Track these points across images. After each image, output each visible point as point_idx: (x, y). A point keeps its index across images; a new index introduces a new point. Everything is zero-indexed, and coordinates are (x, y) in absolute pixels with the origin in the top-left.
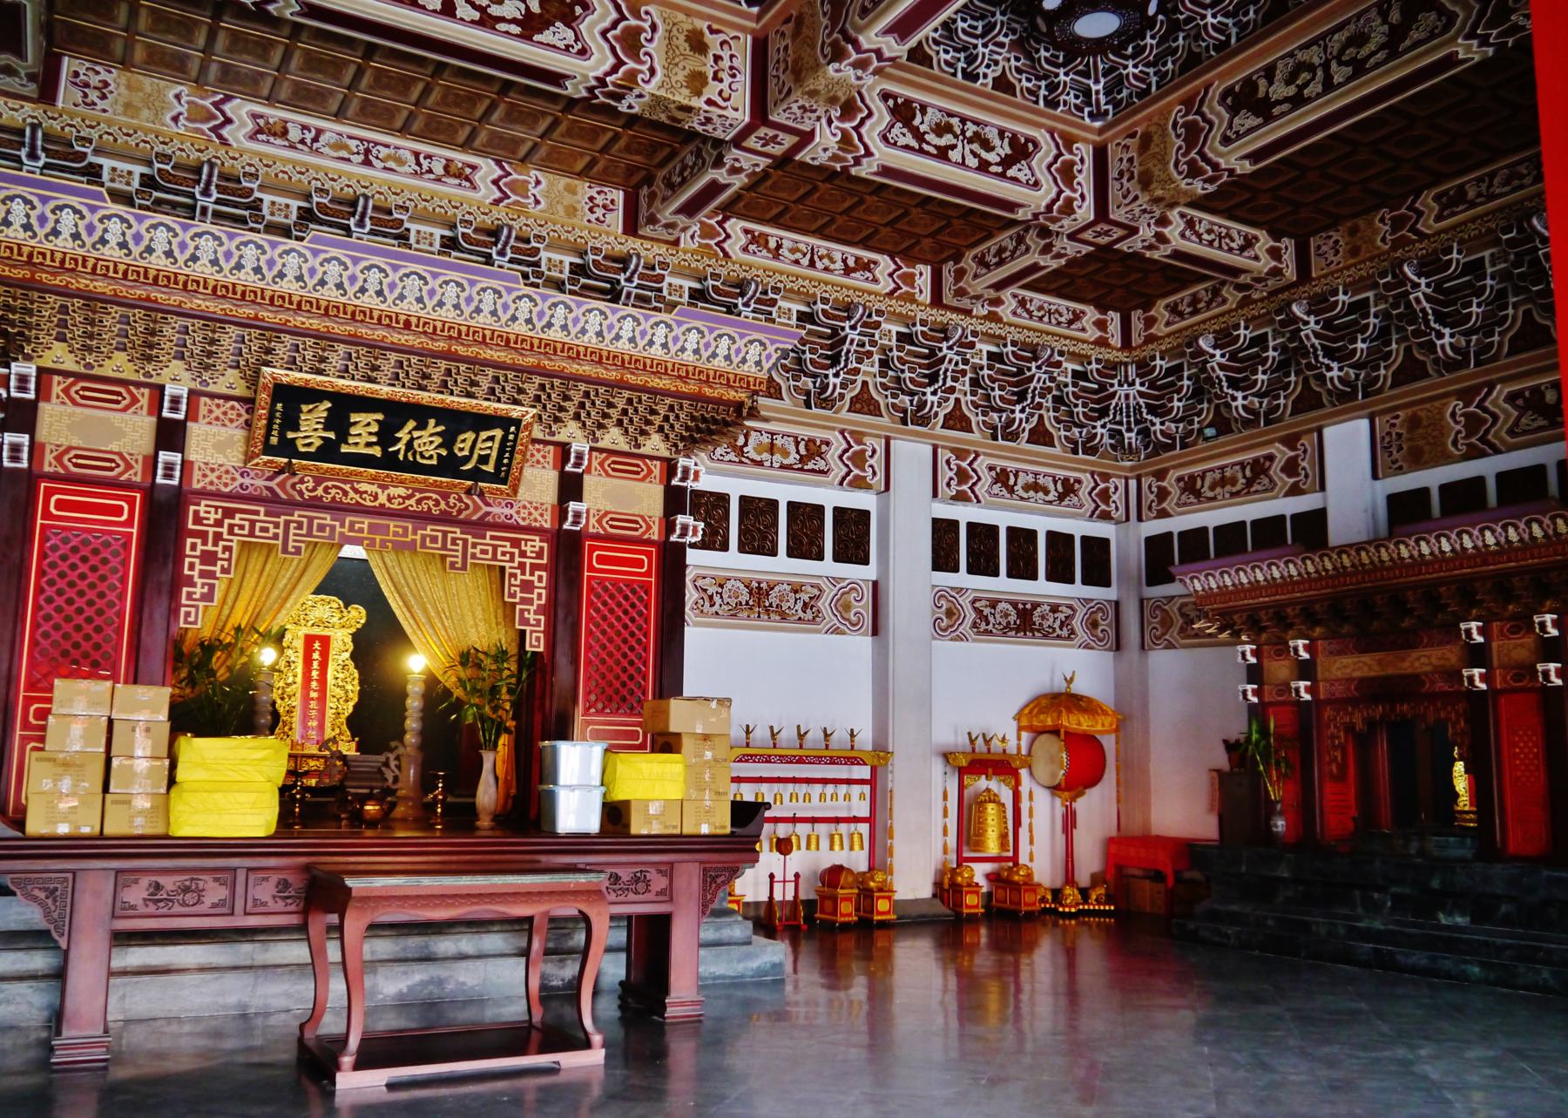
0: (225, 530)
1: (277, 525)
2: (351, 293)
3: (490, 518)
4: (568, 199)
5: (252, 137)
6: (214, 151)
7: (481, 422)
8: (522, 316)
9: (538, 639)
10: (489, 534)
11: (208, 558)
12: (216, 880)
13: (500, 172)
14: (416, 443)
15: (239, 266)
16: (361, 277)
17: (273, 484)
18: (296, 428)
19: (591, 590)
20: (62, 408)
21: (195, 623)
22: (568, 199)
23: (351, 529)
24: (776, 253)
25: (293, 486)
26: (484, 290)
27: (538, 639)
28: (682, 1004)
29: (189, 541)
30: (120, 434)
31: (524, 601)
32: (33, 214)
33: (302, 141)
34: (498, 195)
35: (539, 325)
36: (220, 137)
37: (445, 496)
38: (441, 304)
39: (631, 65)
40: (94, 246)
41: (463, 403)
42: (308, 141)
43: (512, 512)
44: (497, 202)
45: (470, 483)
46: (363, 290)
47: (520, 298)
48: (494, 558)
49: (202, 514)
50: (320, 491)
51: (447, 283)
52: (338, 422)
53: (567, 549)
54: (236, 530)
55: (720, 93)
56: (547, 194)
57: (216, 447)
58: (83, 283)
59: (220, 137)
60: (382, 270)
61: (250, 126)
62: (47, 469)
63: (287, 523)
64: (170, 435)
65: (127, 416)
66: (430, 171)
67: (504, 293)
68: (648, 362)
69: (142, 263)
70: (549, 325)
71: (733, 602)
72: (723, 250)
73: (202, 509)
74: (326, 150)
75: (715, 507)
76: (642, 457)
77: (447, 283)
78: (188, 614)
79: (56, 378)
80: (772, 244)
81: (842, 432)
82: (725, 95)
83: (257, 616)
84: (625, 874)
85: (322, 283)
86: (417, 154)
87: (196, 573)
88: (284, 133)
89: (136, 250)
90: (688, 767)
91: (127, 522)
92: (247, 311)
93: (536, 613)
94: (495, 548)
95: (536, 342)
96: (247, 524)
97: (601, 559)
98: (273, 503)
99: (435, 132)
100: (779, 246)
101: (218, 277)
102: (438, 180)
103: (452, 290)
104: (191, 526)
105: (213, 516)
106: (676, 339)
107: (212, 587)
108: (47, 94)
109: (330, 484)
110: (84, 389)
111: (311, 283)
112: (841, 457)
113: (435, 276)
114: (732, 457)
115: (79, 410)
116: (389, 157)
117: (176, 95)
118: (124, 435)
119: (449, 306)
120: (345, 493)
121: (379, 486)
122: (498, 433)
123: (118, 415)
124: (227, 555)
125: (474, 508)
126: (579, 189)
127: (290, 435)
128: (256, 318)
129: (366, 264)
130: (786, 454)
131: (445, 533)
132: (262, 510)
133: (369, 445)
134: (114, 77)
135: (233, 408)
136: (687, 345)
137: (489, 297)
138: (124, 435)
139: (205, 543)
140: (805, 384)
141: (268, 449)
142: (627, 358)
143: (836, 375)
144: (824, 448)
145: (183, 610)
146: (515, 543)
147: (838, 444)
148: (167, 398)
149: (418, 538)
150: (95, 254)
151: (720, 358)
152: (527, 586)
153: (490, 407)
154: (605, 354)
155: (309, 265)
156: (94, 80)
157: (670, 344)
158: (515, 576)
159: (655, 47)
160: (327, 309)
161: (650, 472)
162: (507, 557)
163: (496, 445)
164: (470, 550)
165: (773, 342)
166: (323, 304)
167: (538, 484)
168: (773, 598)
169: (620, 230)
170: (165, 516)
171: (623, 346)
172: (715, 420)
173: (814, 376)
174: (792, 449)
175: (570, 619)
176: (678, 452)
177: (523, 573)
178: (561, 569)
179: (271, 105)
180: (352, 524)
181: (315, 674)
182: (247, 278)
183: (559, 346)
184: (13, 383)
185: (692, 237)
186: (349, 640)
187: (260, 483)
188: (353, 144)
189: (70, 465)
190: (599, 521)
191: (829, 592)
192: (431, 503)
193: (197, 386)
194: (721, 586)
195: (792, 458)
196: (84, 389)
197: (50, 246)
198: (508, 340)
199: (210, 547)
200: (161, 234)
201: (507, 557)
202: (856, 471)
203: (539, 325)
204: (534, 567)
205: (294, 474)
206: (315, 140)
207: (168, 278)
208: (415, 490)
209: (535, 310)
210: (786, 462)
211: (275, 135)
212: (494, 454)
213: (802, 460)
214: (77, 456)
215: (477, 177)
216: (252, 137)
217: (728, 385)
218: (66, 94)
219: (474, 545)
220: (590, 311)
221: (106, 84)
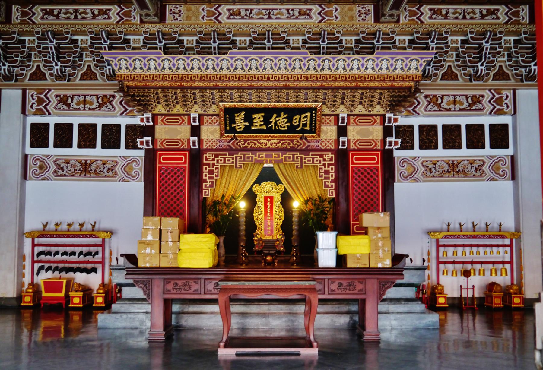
0: (215, 162)
1: (233, 158)
2: (247, 70)
3: (310, 148)
4: (350, 14)
5: (229, 18)
6: (217, 27)
7: (301, 111)
9: (332, 192)
10: (310, 153)
11: (211, 172)
12: (195, 282)
13: (320, 9)
14: (278, 123)
15: (207, 68)
16: (249, 64)
17: (230, 144)
18: (235, 123)
19: (353, 171)
20: (162, 126)
21: (208, 195)
22: (350, 14)
23: (259, 157)
24: (446, 17)
25: (237, 144)
26: (295, 60)
27: (332, 192)
28: (371, 334)
29: (204, 167)
30: (180, 133)
31: (325, 178)
32: (142, 64)
33: (246, 15)
35: (319, 70)
36: (218, 20)
37: (292, 141)
38: (280, 68)
40: (161, 70)
42: (248, 14)
43: (319, 144)
44: (320, 21)
45: (301, 135)
46: (251, 69)
47: (310, 60)
48: (313, 162)
49: (208, 157)
50: (246, 145)
51: (281, 60)
52: (249, 118)
53: (342, 157)
54: (219, 162)
56: (341, 13)
57: (211, 133)
58: (161, 84)
59: (218, 20)
60: (256, 60)
61: (228, 14)
62: (158, 147)
63: (236, 157)
64: (195, 131)
65: (181, 126)
67: (303, 60)
68: (367, 77)
69: (177, 73)
70: (323, 69)
71: (441, 171)
72: (420, 20)
73: (208, 155)
74: (255, 16)
75: (430, 131)
76: (372, 115)
77: (281, 60)
78: (205, 192)
79: (159, 117)
80: (444, 12)
81: (490, 90)
83: (236, 191)
84: (345, 283)
85: (236, 69)
86: (288, 10)
87: (207, 178)
89: (174, 69)
90: (371, 240)
91: (184, 162)
92: (213, 84)
93: (331, 182)
94: (313, 159)
95: (319, 76)
96: (223, 159)
97: (357, 159)
98: (230, 150)
100: (447, 13)
101: (201, 73)
102: (297, 18)
103: (283, 62)
104: (204, 162)
105: (211, 158)
106: (377, 65)
107: (213, 182)
108: (162, 19)
109: (250, 141)
110: (168, 119)
111: (232, 69)
112: (490, 102)
113: (276, 58)
114: (436, 108)
115: (167, 126)
116: (278, 14)
117: (203, 9)
118: (181, 133)
119: (283, 69)
120: (255, 144)
121: (267, 140)
122: (308, 114)
123: (179, 126)
124: (217, 171)
126: (354, 9)
127: (233, 126)
128: (216, 85)
129: (250, 58)
130: (462, 104)
131: (294, 155)
132: (227, 153)
133: (261, 125)
134: (183, 8)
135: (215, 118)
136: (383, 67)
137: (297, 62)
138: (181, 133)
139: (209, 167)
140: (469, 71)
141: (227, 132)
142: (357, 76)
143: (482, 65)
144: (481, 99)
145: (204, 191)
146: (321, 156)
147: (488, 95)
148: (191, 118)
149: (283, 158)
150: (162, 73)
151: (399, 69)
152: (327, 172)
153: (302, 104)
154: (347, 76)
155: (230, 63)
156: (177, 11)
157: (375, 67)
158: (322, 169)
160: (239, 78)
161: (375, 121)
162: (318, 162)
163: (309, 119)
164: (304, 161)
165: (422, 58)
166: (238, 76)
167: (329, 132)
168: (460, 167)
169: (373, 22)
170: (196, 158)
171: (355, 72)
172: (402, 97)
173: (473, 67)
174: (465, 101)
175: (344, 184)
176: (388, 112)
177: (325, 167)
178: (340, 163)
179: (234, 4)
180: (259, 155)
181: (269, 210)
182: (210, 72)
183: (328, 76)
184: (145, 121)
185: (405, 18)
186: (279, 197)
187: (226, 144)
188: (264, 11)
189: (165, 145)
190: (355, 144)
191: (488, 163)
192: (287, 144)
193: (202, 112)
194: (435, 164)
195: (465, 105)
196: (168, 119)
197: (149, 73)
198: (307, 78)
199: (211, 168)
200: (181, 62)
201: (318, 162)
202: (498, 107)
203: (319, 70)
204: (329, 165)
205: (237, 139)
206: (250, 13)
207: (185, 77)
208: (281, 140)
209: (316, 64)
210: (462, 107)
211: (236, 15)
212: (308, 123)
213: (470, 105)
214: (167, 142)
215: (312, 14)
216: (229, 18)
217: (403, 80)
218: (169, 18)
219: (305, 158)
220: (339, 60)
221: (180, 11)
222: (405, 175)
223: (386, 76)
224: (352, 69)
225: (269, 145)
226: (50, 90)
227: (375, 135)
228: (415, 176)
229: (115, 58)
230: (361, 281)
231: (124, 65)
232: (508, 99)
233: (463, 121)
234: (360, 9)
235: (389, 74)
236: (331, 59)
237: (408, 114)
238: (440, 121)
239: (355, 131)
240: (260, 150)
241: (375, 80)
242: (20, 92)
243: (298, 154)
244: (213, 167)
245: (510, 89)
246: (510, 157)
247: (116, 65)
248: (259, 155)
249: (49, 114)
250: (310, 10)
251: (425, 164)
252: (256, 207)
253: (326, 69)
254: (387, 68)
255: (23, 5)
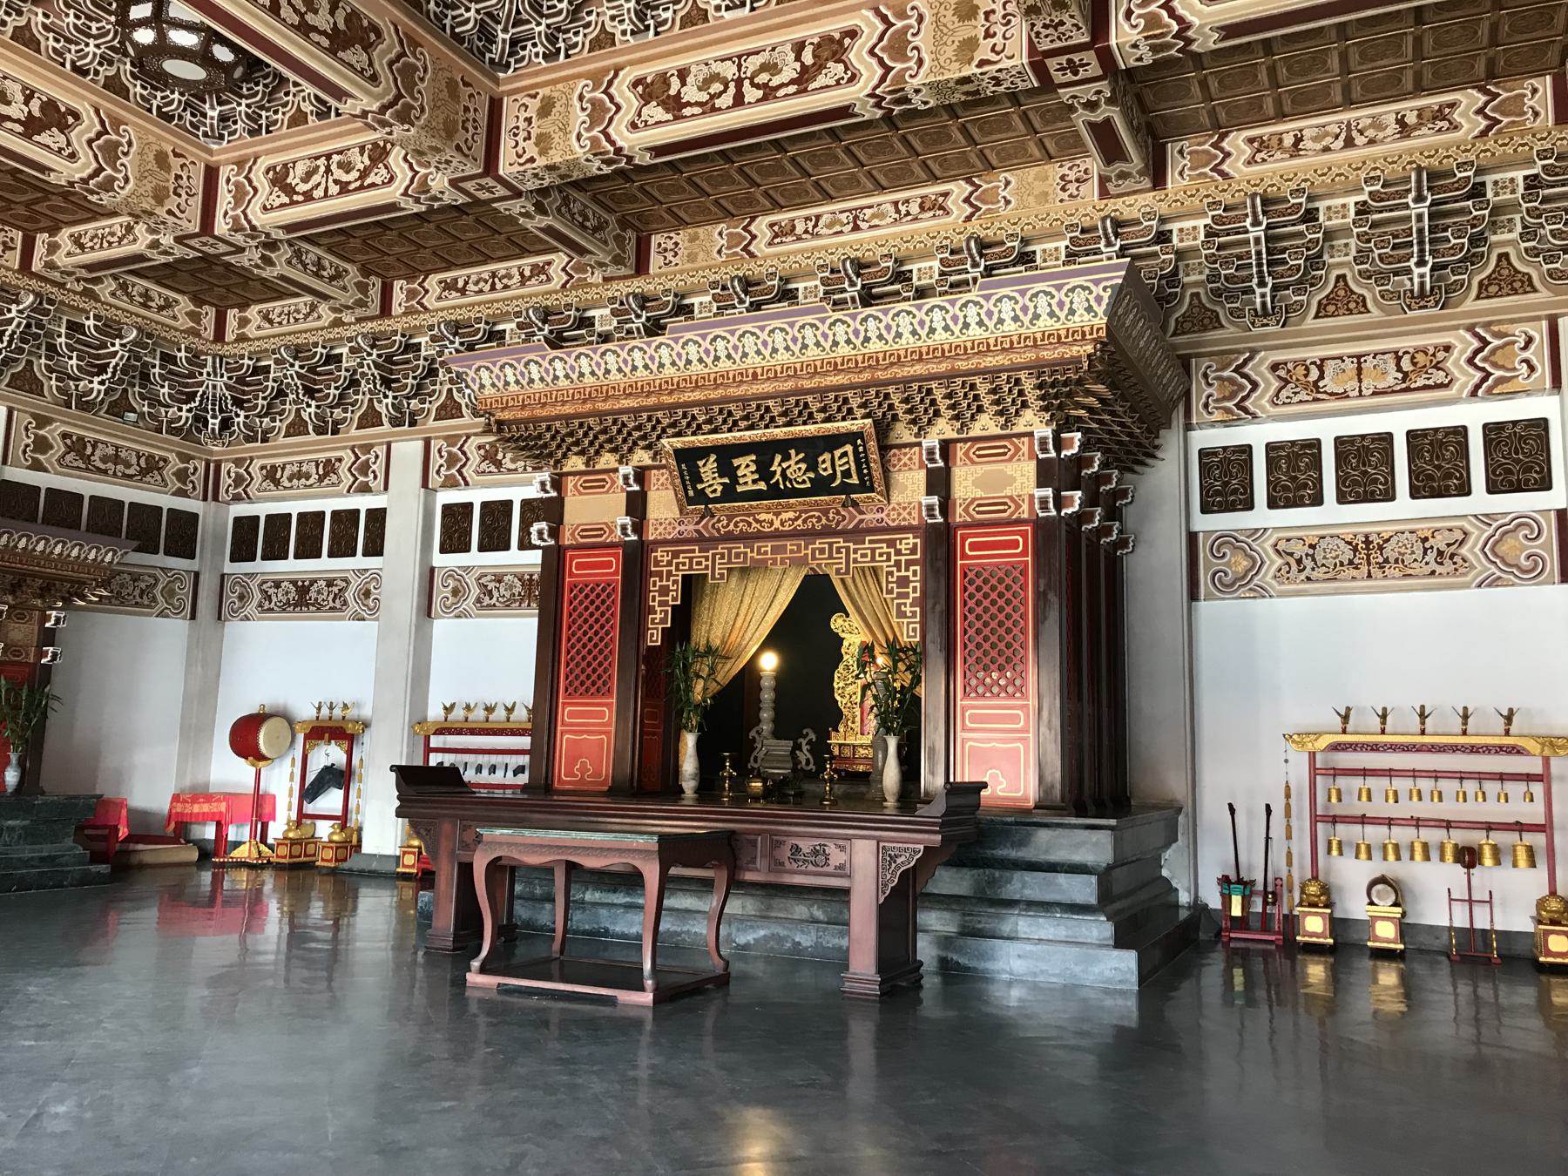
4: (1039, 187)
7: (832, 442)
8: (841, 339)
13: (970, 189)
17: (699, 527)
18: (702, 482)
27: (914, 630)
31: (900, 596)
33: (806, 232)
34: (969, 210)
37: (825, 513)
39: (899, 66)
41: (810, 429)
44: (968, 219)
47: (834, 324)
48: (873, 559)
50: (731, 527)
52: (727, 469)
53: (940, 542)
55: (993, 50)
57: (663, 505)
61: (769, 234)
63: (714, 555)
66: (908, 214)
70: (867, 339)
74: (825, 231)
81: (1470, 329)
82: (998, 48)
86: (896, 204)
88: (794, 227)
94: (873, 550)
97: (973, 547)
98: (702, 541)
99: (900, 179)
108: (641, 268)
113: (762, 329)
116: (874, 216)
117: (716, 235)
120: (750, 524)
122: (849, 448)
125: (851, 519)
127: (700, 487)
131: (831, 544)
133: (754, 482)
134: (682, 237)
136: (1003, 316)
141: (690, 501)
142: (946, 347)
146: (891, 544)
147: (1464, 343)
152: (904, 582)
154: (924, 350)
156: (670, 245)
158: (891, 573)
159: (922, 40)
168: (1390, 551)
171: (941, 336)
175: (938, 608)
177: (899, 570)
180: (759, 548)
185: (1181, 174)
188: (843, 217)
191: (1478, 536)
195: (1392, 377)
203: (858, 343)
204: (909, 563)
205: (713, 516)
206: (815, 226)
210: (1381, 386)
211: (786, 235)
215: (949, 203)
218: (655, 261)
219: (855, 551)
221: (676, 244)
222: (1226, 580)
223: (1015, 339)
224: (932, 331)
225: (777, 524)
226: (468, 437)
227: (1018, 484)
228: (1256, 581)
229: (470, 367)
230: (841, 843)
231: (492, 379)
232: (1533, 347)
233: (1397, 423)
234: (1065, 170)
235: (1022, 331)
236: (880, 315)
237: (1225, 417)
238: (1327, 430)
239: (971, 479)
240: (760, 536)
241: (989, 350)
242: (420, 444)
243: (840, 542)
245: (1538, 318)
246: (1553, 515)
247: (473, 380)
248: (759, 548)
249: (467, 484)
250: (946, 195)
251: (1282, 546)
252: (841, 667)
253: (874, 339)
254: (1016, 319)
255: (410, 278)
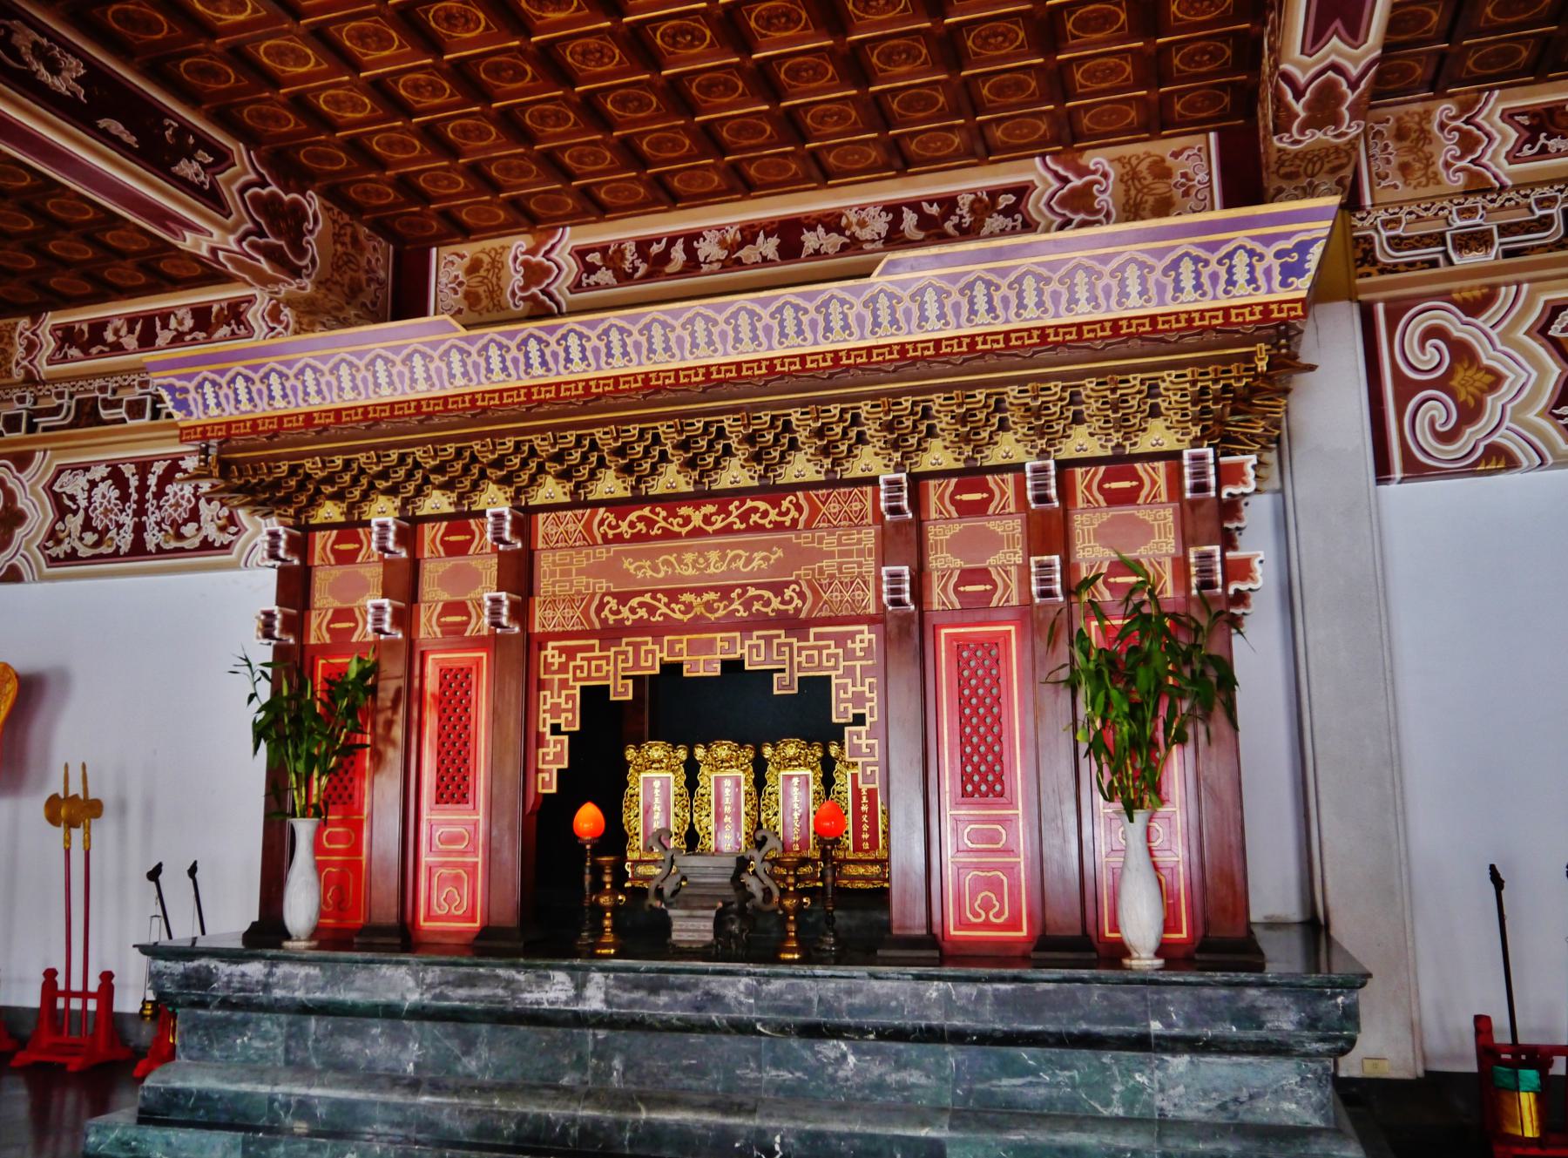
10: (813, 631)
105: (556, 661)
146: (841, 640)
149: (746, 651)
180: (671, 644)
219: (800, 649)
244: (574, 688)
